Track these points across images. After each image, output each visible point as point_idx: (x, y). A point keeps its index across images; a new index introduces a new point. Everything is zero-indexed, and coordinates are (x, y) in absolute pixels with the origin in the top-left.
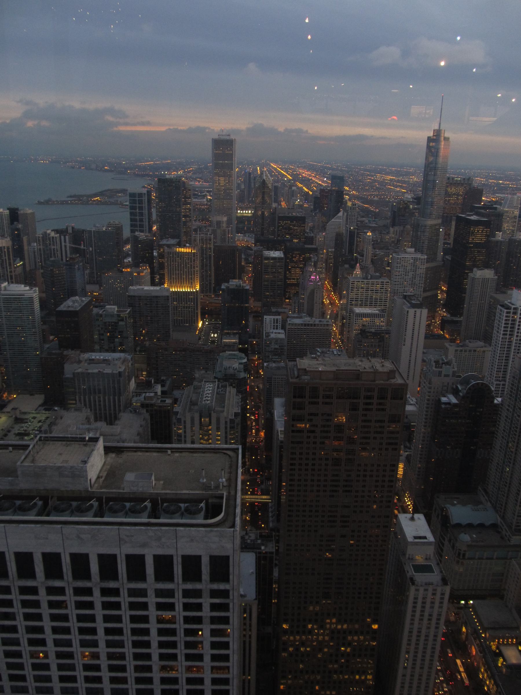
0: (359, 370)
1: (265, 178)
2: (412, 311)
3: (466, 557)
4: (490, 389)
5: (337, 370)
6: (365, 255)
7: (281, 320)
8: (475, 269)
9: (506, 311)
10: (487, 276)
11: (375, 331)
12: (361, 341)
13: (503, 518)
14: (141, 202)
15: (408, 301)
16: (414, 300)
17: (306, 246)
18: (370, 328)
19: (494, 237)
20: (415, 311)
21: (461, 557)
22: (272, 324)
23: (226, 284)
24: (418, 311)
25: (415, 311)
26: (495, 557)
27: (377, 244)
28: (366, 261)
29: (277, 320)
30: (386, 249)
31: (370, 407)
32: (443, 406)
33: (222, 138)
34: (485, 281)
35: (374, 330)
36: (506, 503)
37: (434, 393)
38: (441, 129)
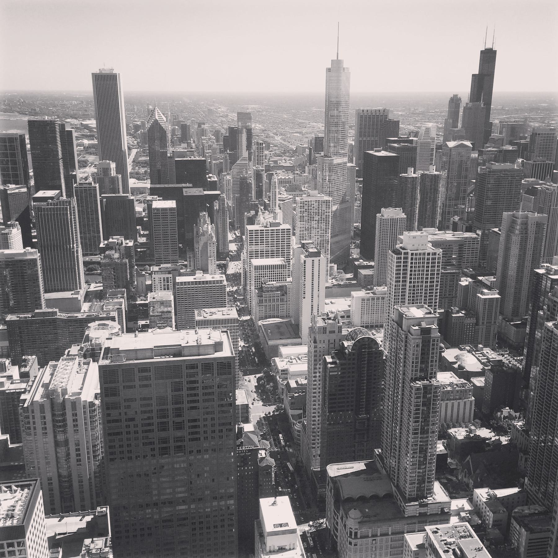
0: (180, 345)
1: (157, 118)
2: (309, 260)
3: (359, 536)
4: (376, 343)
5: (155, 347)
7: (172, 279)
8: (383, 209)
9: (396, 256)
12: (262, 296)
13: (397, 487)
14: (13, 148)
17: (206, 193)
18: (272, 281)
19: (407, 173)
20: (313, 261)
21: (353, 537)
22: (162, 284)
23: (106, 242)
24: (316, 259)
25: (313, 261)
26: (390, 533)
29: (167, 278)
31: (195, 385)
32: (329, 366)
33: (103, 72)
34: (393, 221)
35: (275, 282)
36: (398, 470)
37: (320, 352)
38: (339, 59)
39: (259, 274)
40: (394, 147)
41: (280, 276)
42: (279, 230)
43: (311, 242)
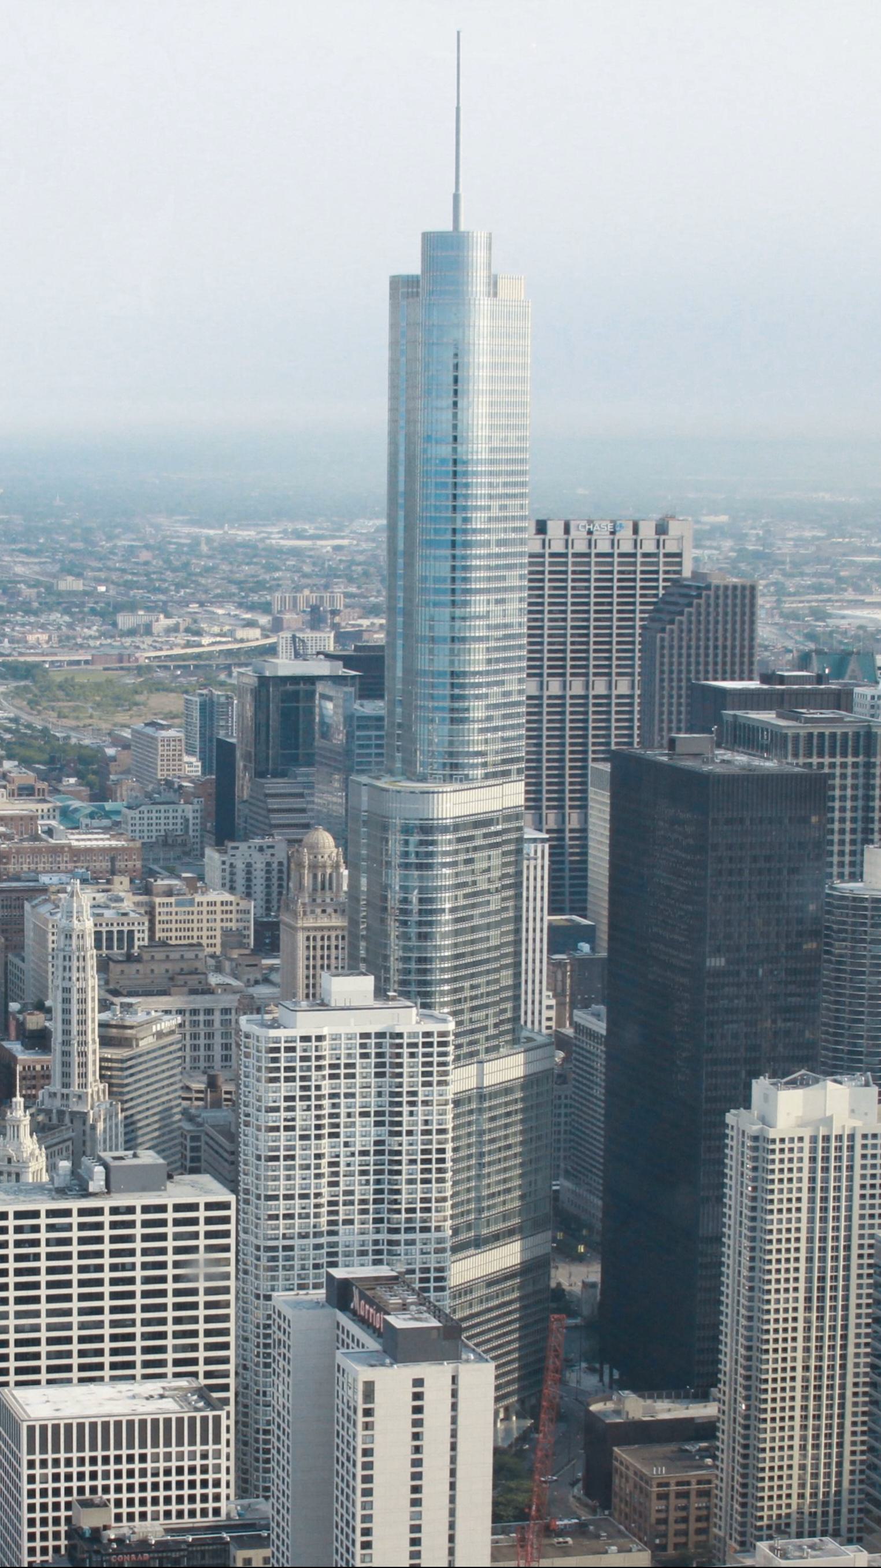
6: (57, 1038)
8: (760, 1086)
10: (843, 1122)
11: (168, 1531)
15: (363, 1322)
16: (404, 1307)
18: (131, 1517)
25: (418, 1382)
27: (130, 958)
28: (66, 1075)
30: (193, 992)
39: (56, 1478)
40: (765, 727)
41: (168, 1486)
42: (163, 1208)
43: (384, 1271)
